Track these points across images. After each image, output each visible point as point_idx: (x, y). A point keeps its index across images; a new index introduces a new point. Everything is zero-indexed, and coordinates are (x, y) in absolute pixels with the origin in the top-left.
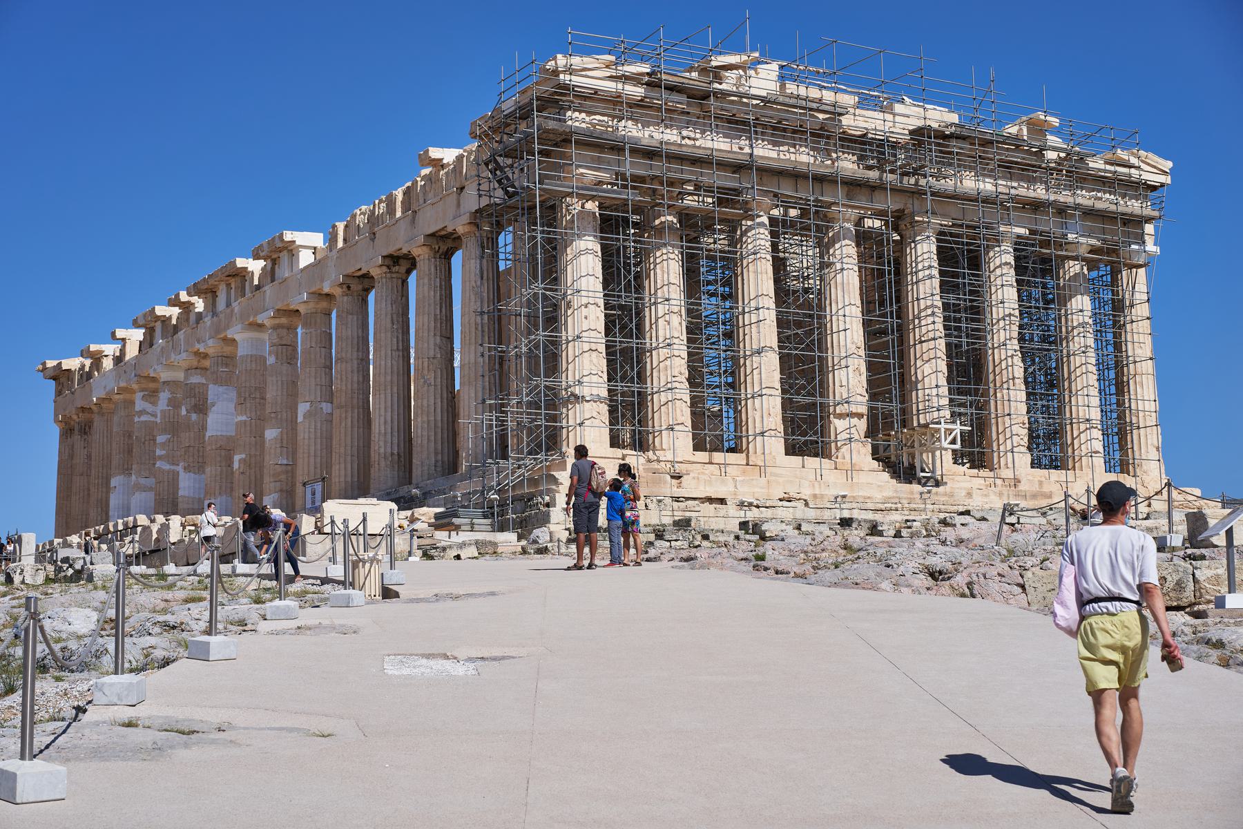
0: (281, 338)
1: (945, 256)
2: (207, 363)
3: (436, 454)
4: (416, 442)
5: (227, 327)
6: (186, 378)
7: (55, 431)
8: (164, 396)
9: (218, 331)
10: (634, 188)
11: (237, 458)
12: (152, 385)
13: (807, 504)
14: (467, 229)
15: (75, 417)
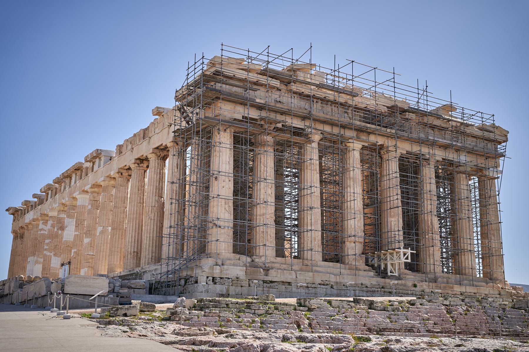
0: (94, 197)
1: (402, 168)
2: (66, 208)
3: (152, 253)
4: (144, 246)
5: (74, 192)
6: (58, 215)
7: (11, 236)
8: (50, 223)
9: (70, 194)
10: (250, 123)
11: (73, 251)
12: (47, 218)
13: (332, 287)
14: (172, 144)
15: (19, 231)
